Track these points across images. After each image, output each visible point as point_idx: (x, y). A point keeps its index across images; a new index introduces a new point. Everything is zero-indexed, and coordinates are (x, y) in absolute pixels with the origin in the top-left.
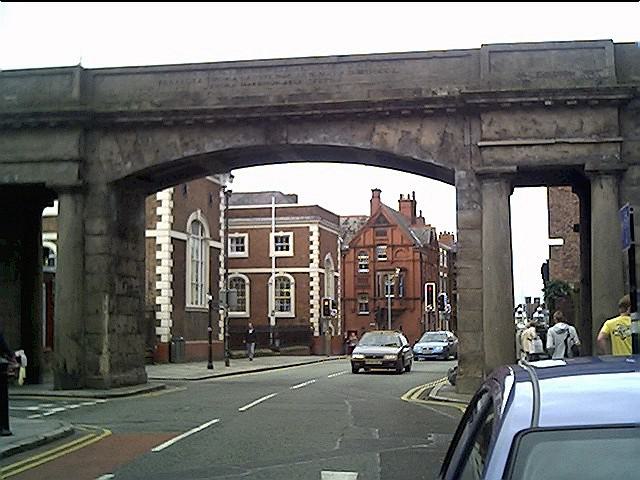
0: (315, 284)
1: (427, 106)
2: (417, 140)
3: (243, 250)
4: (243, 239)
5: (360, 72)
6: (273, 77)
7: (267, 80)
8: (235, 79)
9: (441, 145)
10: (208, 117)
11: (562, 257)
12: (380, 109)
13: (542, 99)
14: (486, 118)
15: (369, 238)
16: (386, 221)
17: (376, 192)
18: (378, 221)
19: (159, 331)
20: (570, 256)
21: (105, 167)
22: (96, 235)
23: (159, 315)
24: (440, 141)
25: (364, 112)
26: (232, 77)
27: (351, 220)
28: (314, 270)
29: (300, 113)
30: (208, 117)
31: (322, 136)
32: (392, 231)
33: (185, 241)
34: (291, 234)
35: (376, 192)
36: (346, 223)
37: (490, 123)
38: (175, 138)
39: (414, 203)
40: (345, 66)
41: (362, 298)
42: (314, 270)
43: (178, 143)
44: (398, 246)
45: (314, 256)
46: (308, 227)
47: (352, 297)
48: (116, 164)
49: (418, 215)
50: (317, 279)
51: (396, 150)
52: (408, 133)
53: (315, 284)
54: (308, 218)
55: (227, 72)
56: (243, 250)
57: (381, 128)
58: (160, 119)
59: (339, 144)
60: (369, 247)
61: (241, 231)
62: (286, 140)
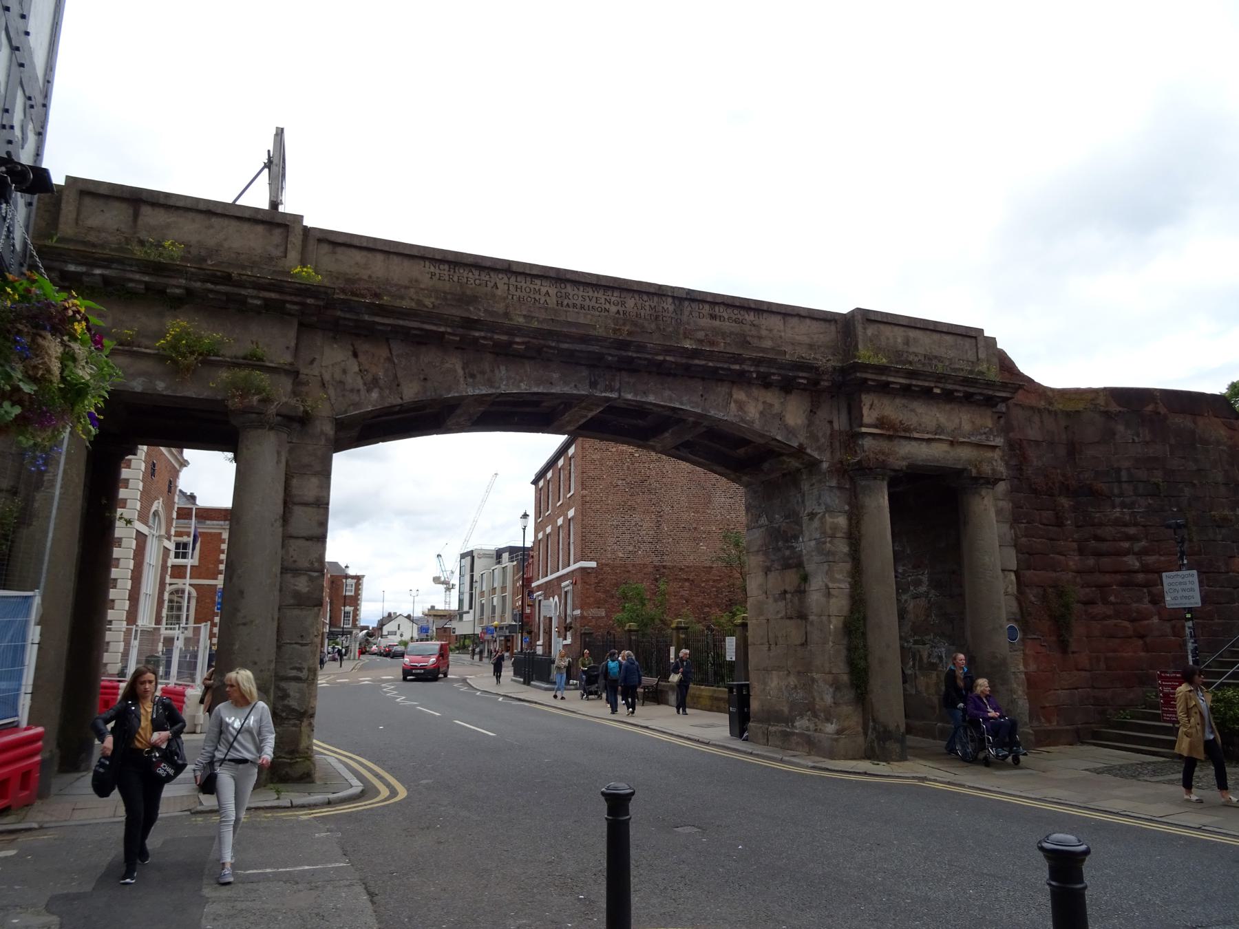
1: (801, 374)
2: (781, 417)
5: (713, 317)
6: (603, 301)
7: (593, 303)
8: (547, 293)
9: (809, 426)
10: (518, 340)
11: (593, 580)
12: (746, 367)
13: (932, 385)
14: (867, 399)
19: (107, 657)
20: (603, 580)
21: (331, 392)
22: (306, 504)
24: (806, 422)
25: (729, 369)
26: (544, 290)
29: (649, 356)
30: (518, 340)
31: (667, 393)
33: (146, 536)
37: (872, 405)
38: (455, 363)
40: (694, 305)
43: (460, 372)
46: (221, 534)
48: (352, 391)
51: (757, 426)
52: (771, 405)
55: (538, 282)
57: (739, 395)
58: (442, 329)
59: (688, 408)
62: (619, 391)
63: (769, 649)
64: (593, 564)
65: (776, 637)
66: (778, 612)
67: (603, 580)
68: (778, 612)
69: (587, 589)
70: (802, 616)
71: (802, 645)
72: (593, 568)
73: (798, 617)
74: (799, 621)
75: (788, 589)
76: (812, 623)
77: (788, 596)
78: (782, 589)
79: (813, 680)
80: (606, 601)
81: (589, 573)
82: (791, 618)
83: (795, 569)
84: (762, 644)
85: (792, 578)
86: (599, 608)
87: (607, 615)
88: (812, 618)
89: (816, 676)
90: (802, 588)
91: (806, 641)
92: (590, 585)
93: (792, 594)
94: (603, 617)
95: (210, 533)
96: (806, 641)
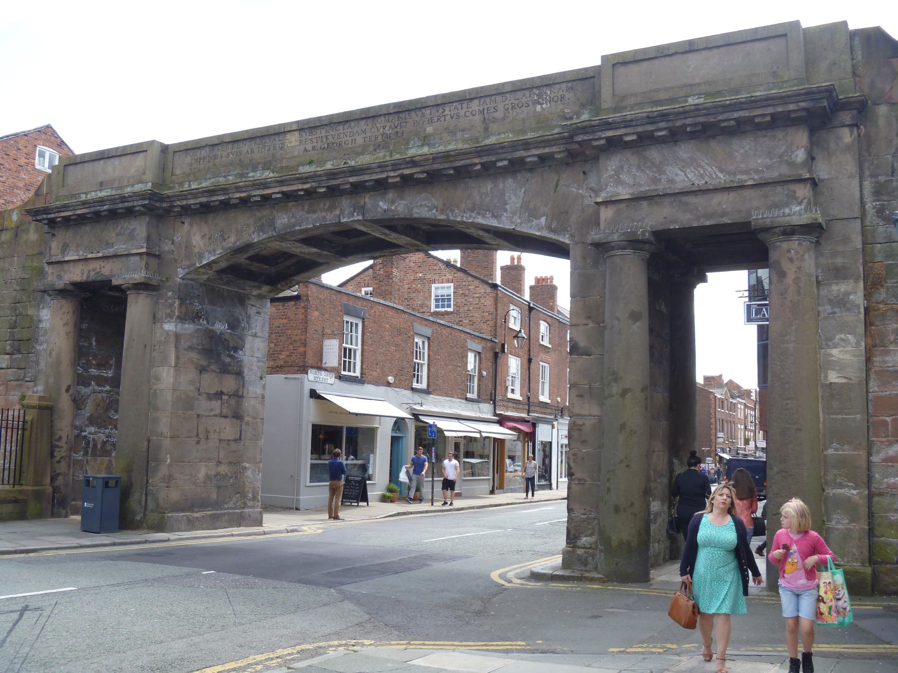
63: (198, 442)
65: (207, 432)
66: (211, 410)
68: (211, 410)
70: (238, 416)
71: (236, 440)
73: (233, 417)
74: (235, 420)
75: (225, 390)
76: (247, 424)
77: (225, 397)
78: (219, 390)
79: (245, 468)
82: (226, 417)
83: (233, 376)
84: (190, 437)
85: (229, 383)
88: (247, 419)
89: (247, 465)
90: (240, 393)
91: (240, 437)
93: (230, 396)
96: (240, 437)
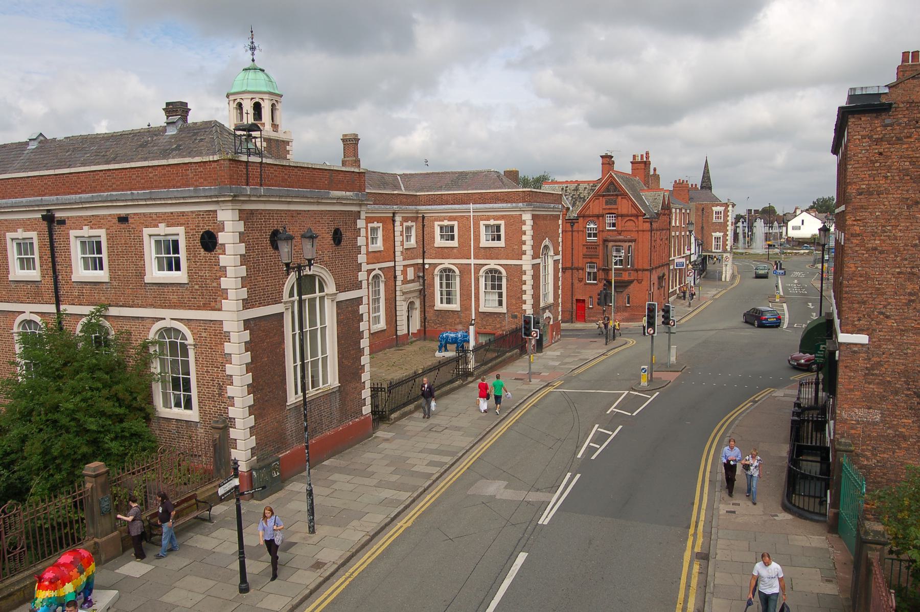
0: (528, 278)
3: (452, 238)
4: (452, 228)
11: (861, 364)
15: (597, 207)
16: (615, 189)
17: (608, 160)
18: (608, 190)
20: (879, 364)
23: (233, 433)
27: (582, 186)
28: (526, 262)
32: (622, 198)
34: (502, 223)
35: (608, 160)
36: (576, 189)
39: (647, 164)
41: (590, 267)
42: (526, 262)
44: (627, 216)
45: (528, 248)
47: (580, 265)
49: (652, 172)
50: (530, 273)
53: (528, 278)
54: (520, 204)
56: (452, 238)
60: (598, 216)
61: (451, 219)
64: (863, 339)
67: (879, 364)
69: (850, 377)
72: (862, 345)
80: (883, 398)
81: (855, 352)
86: (869, 408)
87: (883, 420)
92: (856, 371)
94: (875, 424)
95: (512, 216)
